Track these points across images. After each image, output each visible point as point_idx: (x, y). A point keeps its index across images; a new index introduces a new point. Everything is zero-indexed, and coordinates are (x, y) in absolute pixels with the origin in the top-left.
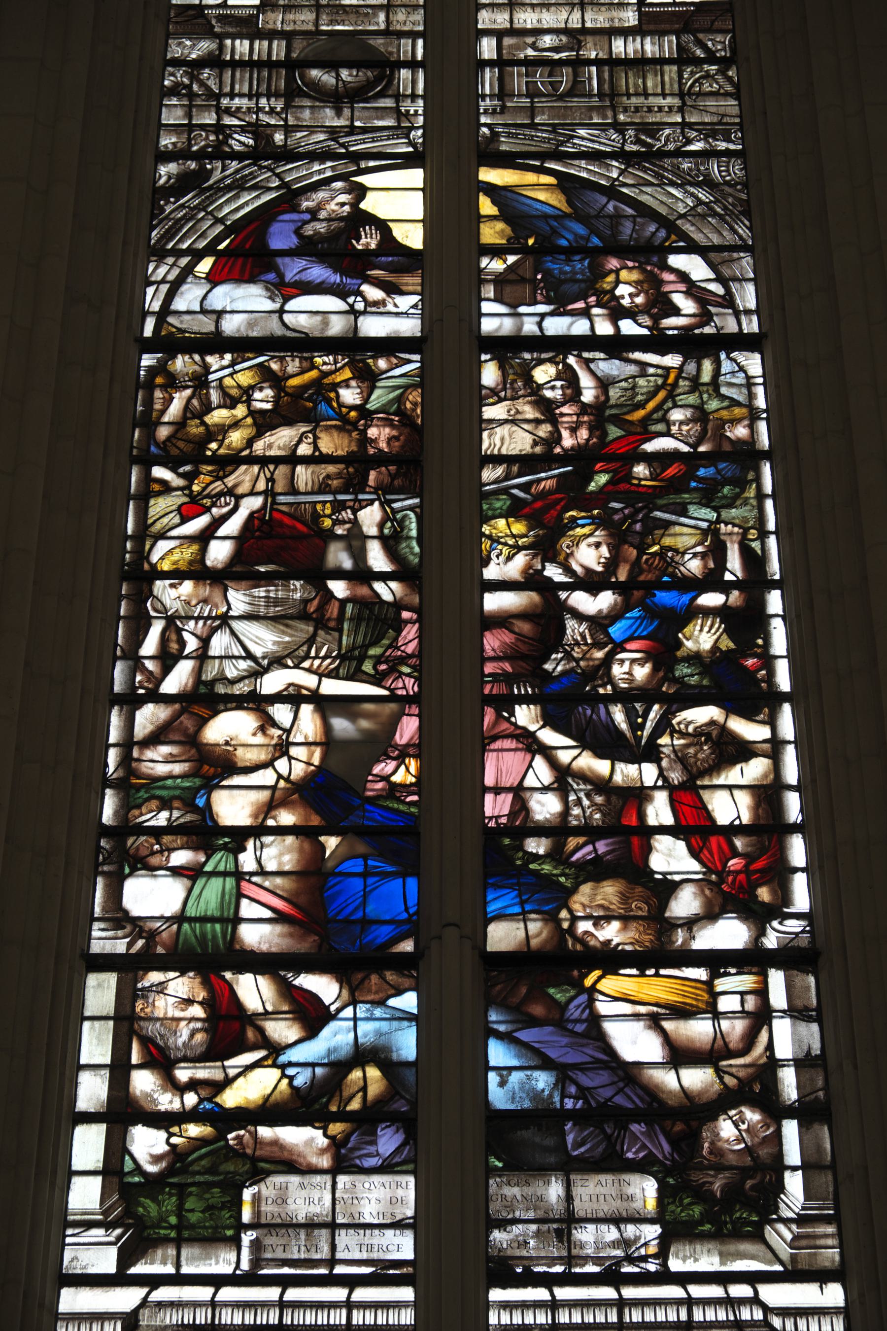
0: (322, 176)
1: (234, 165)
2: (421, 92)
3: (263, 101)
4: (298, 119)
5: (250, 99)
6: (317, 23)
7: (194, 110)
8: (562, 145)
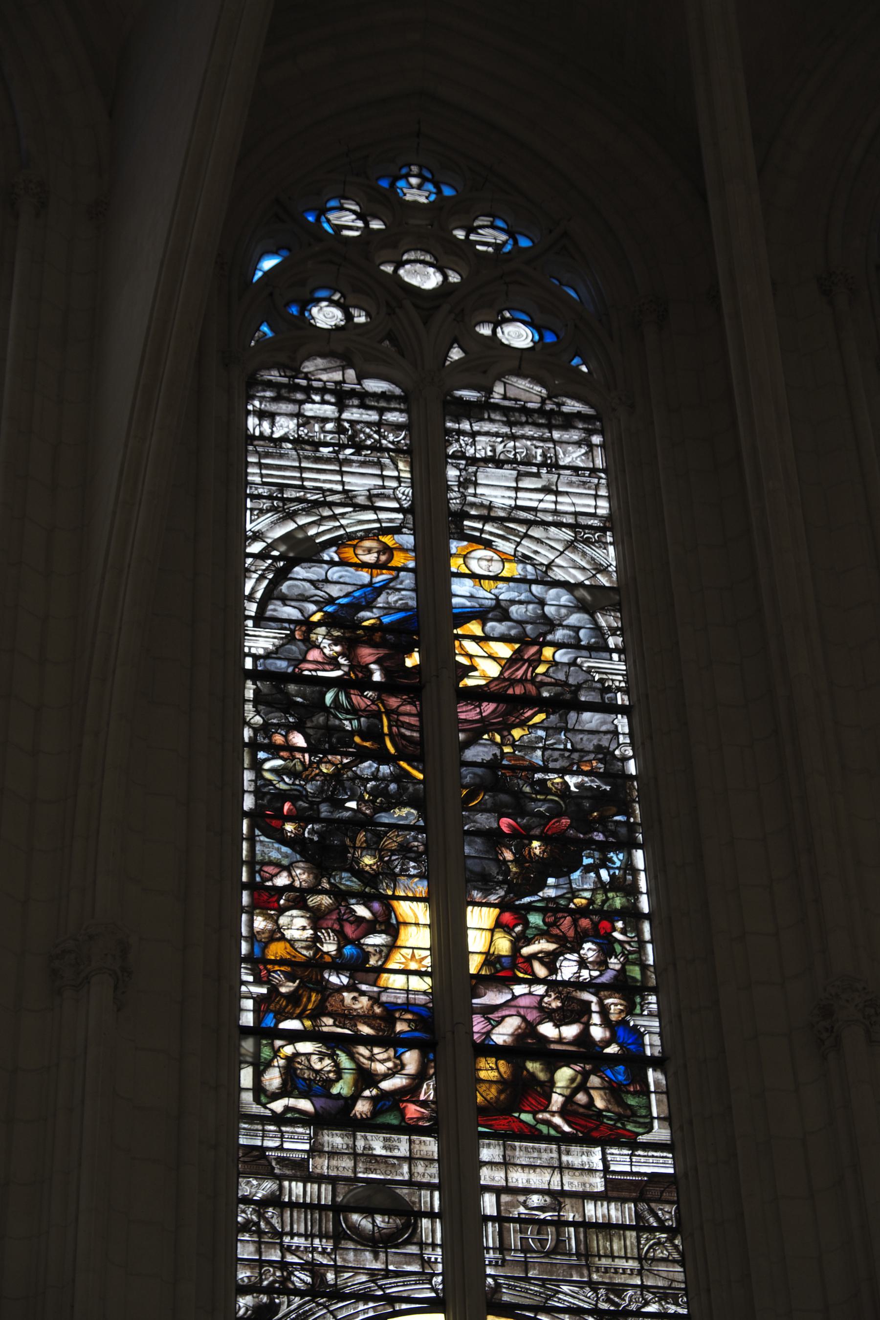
0: (366, 1316)
1: (297, 1301)
2: (439, 1241)
3: (317, 1241)
4: (344, 1260)
5: (306, 1240)
6: (355, 1172)
7: (263, 1246)
8: (549, 1299)
